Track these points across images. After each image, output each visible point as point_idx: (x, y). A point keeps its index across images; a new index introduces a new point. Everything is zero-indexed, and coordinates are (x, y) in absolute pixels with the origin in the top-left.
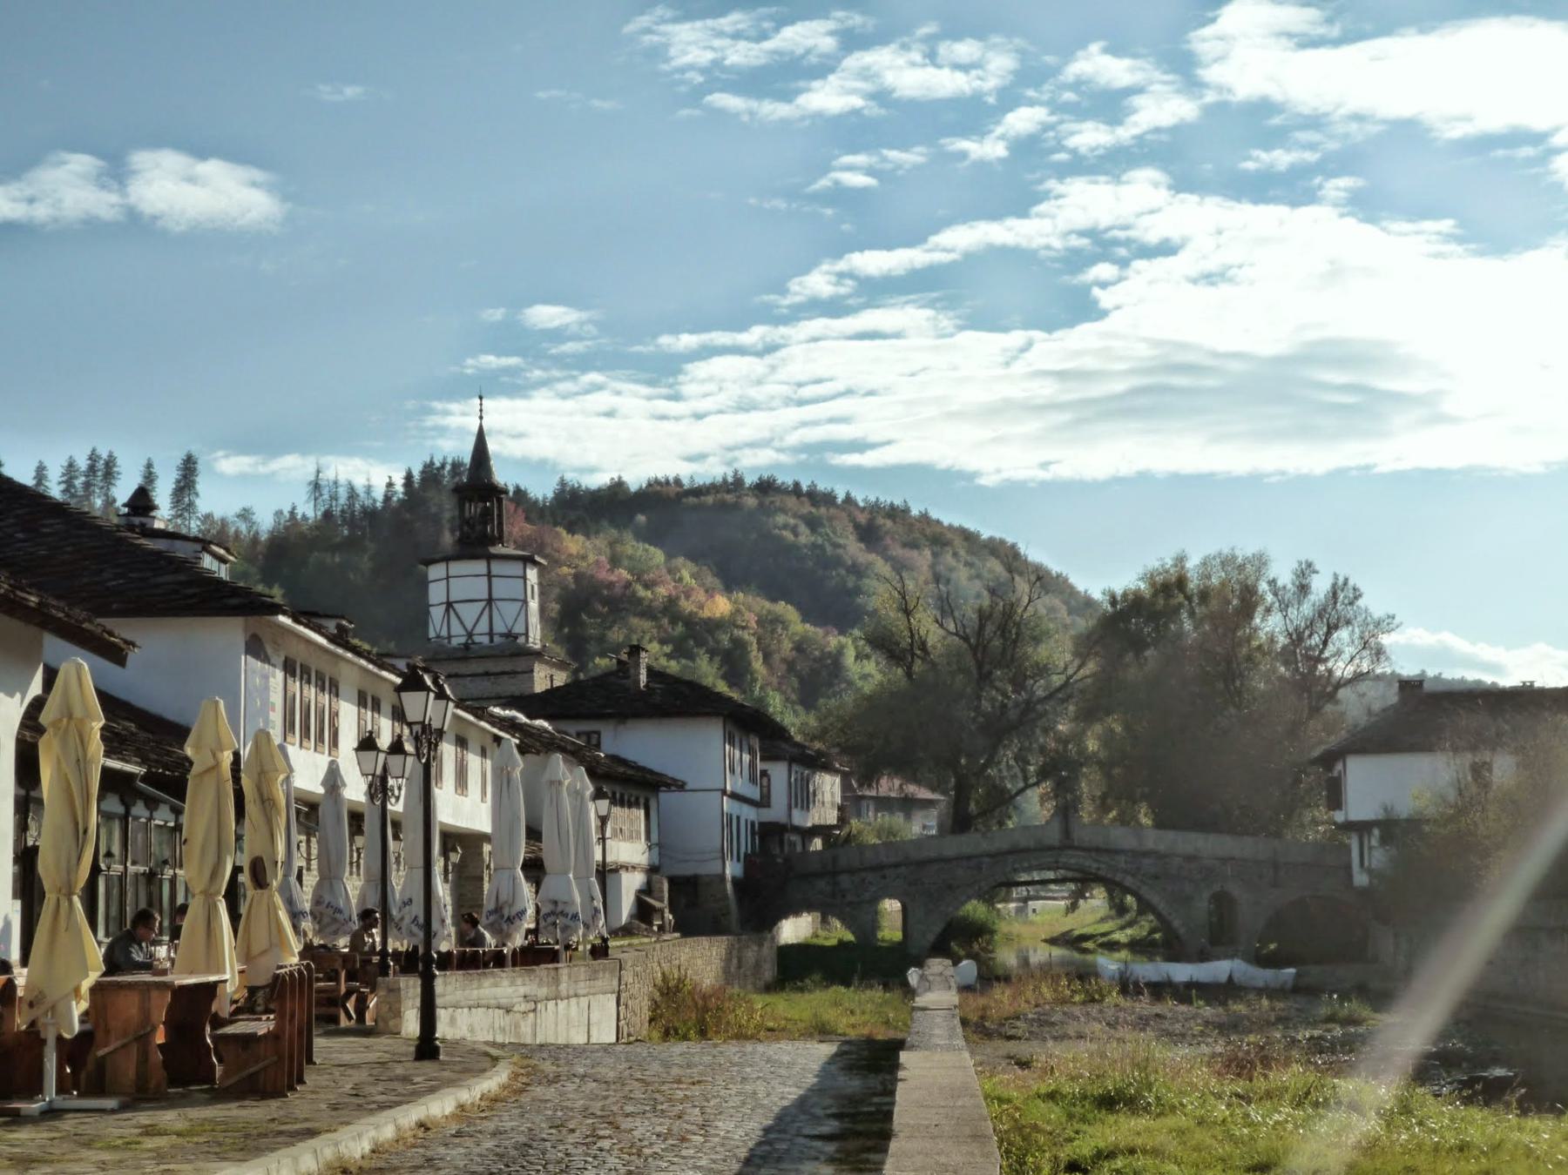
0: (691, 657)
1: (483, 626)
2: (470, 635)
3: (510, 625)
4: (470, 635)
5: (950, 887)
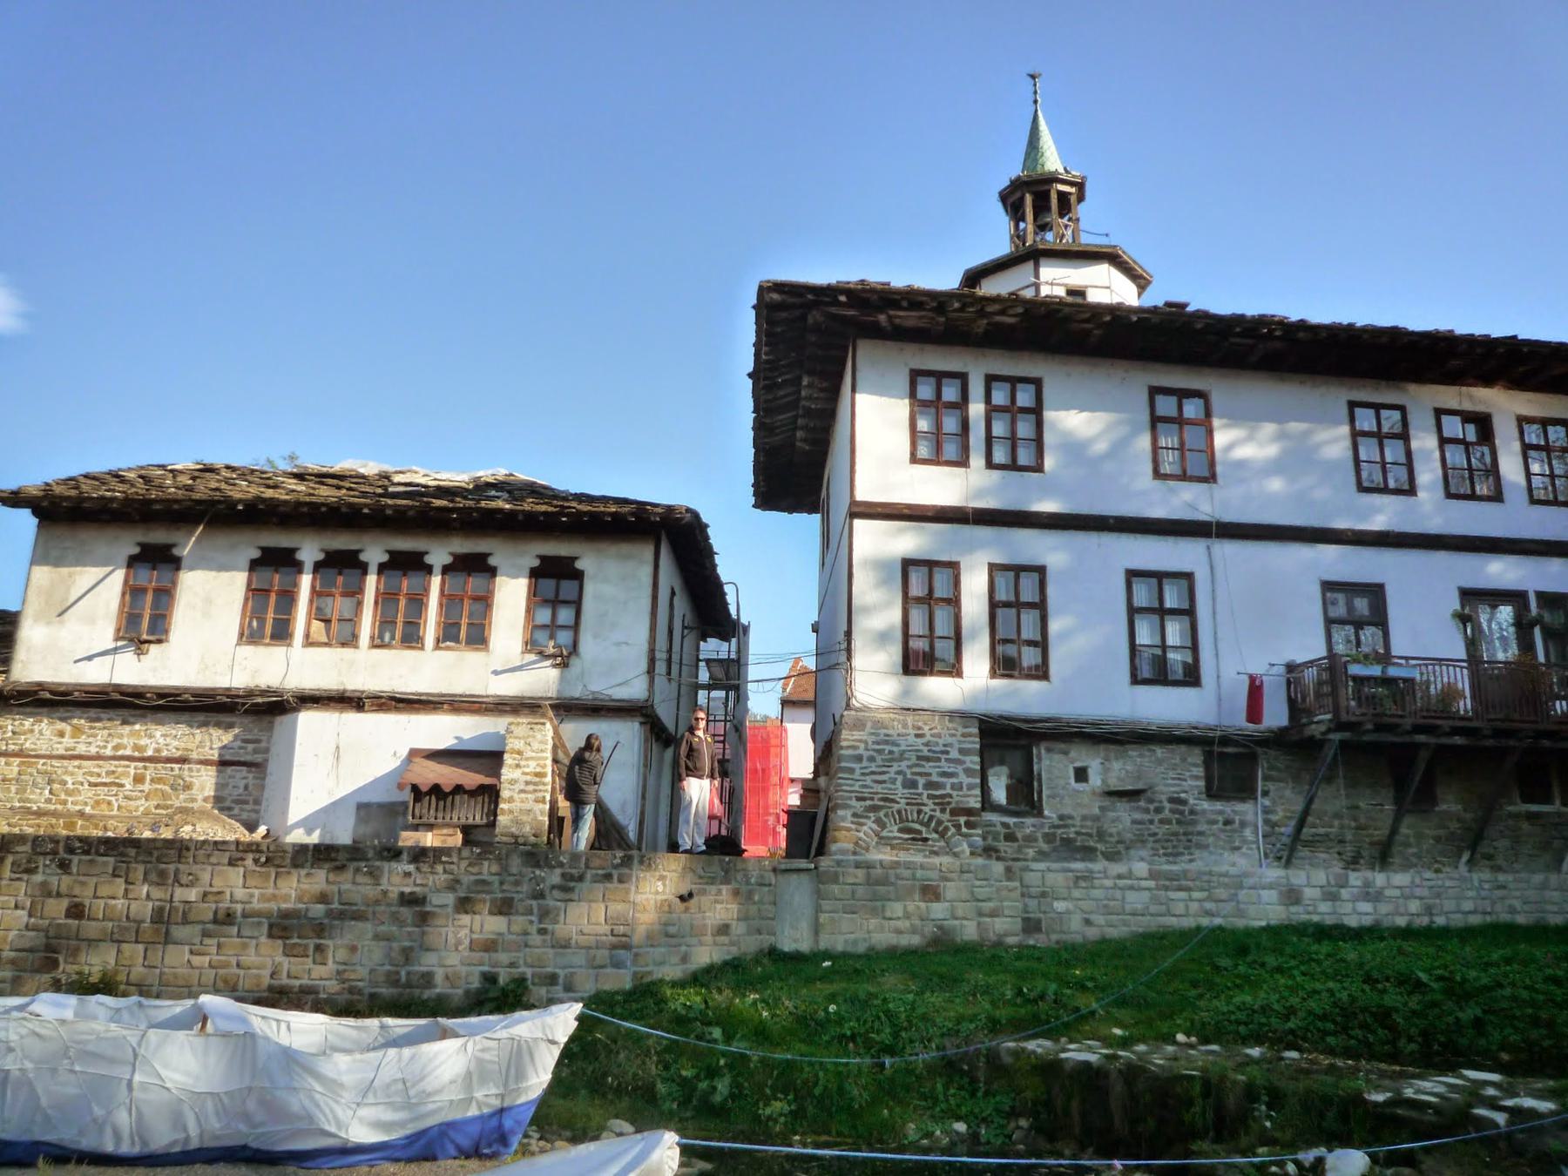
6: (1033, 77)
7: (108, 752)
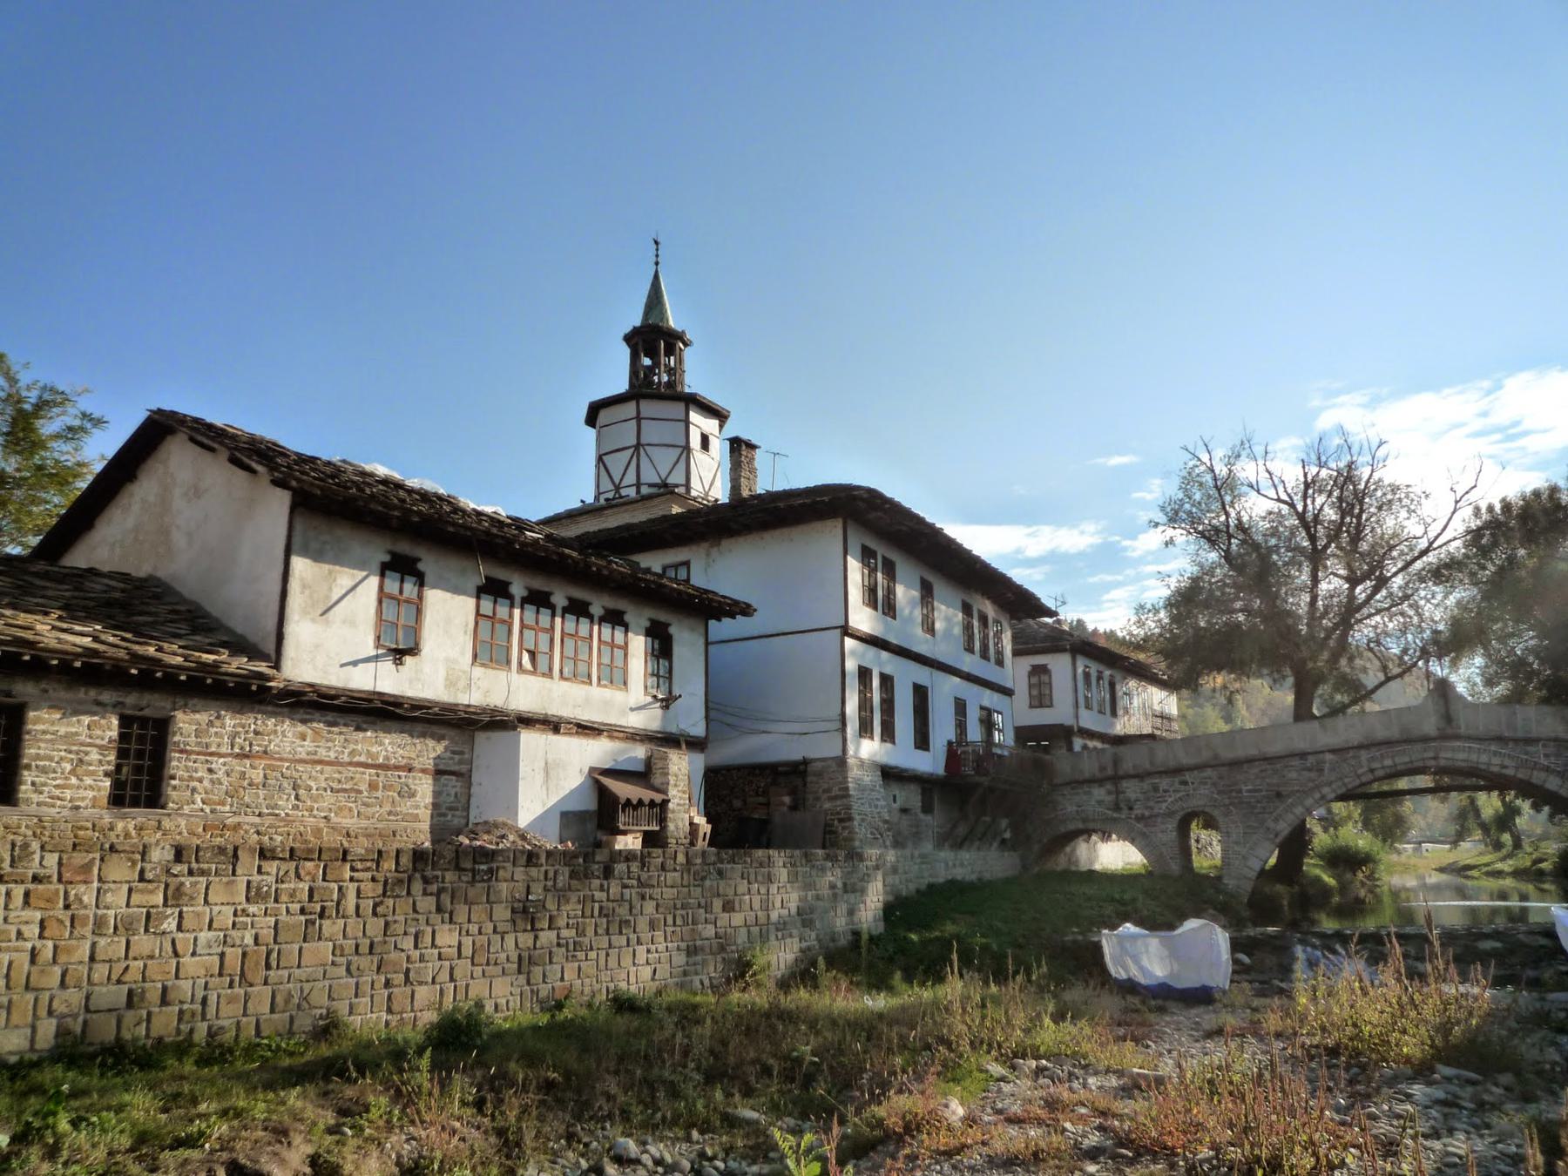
0: (1201, 706)
1: (631, 478)
2: (617, 488)
3: (663, 477)
4: (617, 488)
5: (1279, 795)
6: (656, 243)
7: (346, 759)
